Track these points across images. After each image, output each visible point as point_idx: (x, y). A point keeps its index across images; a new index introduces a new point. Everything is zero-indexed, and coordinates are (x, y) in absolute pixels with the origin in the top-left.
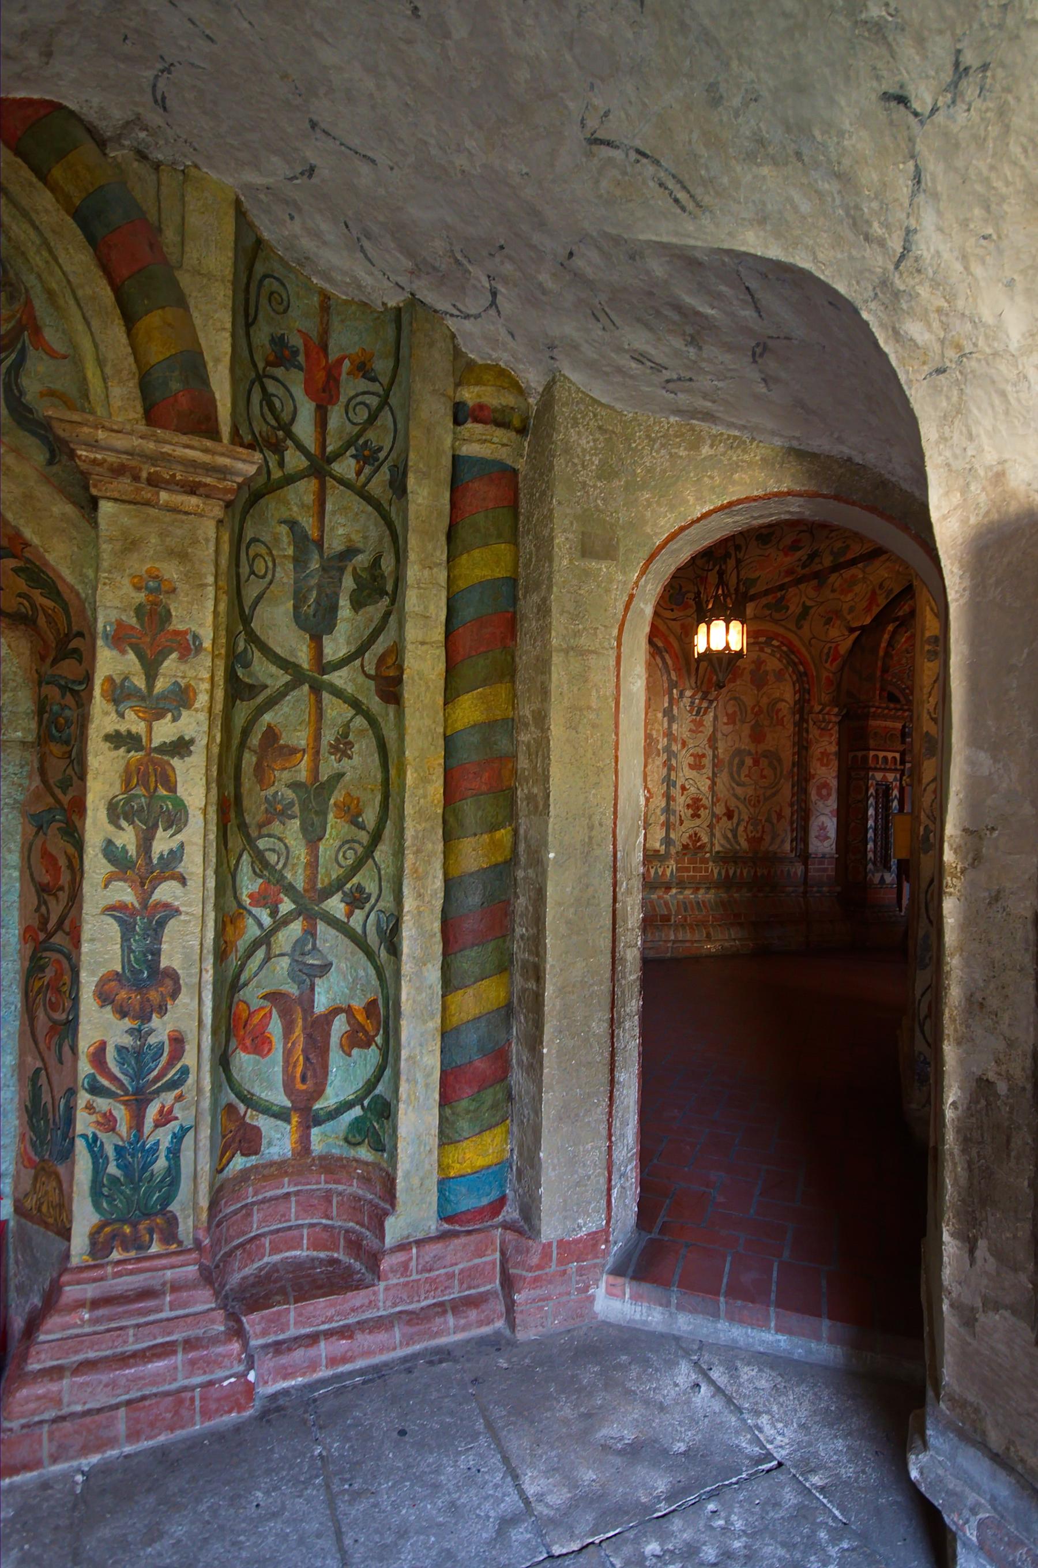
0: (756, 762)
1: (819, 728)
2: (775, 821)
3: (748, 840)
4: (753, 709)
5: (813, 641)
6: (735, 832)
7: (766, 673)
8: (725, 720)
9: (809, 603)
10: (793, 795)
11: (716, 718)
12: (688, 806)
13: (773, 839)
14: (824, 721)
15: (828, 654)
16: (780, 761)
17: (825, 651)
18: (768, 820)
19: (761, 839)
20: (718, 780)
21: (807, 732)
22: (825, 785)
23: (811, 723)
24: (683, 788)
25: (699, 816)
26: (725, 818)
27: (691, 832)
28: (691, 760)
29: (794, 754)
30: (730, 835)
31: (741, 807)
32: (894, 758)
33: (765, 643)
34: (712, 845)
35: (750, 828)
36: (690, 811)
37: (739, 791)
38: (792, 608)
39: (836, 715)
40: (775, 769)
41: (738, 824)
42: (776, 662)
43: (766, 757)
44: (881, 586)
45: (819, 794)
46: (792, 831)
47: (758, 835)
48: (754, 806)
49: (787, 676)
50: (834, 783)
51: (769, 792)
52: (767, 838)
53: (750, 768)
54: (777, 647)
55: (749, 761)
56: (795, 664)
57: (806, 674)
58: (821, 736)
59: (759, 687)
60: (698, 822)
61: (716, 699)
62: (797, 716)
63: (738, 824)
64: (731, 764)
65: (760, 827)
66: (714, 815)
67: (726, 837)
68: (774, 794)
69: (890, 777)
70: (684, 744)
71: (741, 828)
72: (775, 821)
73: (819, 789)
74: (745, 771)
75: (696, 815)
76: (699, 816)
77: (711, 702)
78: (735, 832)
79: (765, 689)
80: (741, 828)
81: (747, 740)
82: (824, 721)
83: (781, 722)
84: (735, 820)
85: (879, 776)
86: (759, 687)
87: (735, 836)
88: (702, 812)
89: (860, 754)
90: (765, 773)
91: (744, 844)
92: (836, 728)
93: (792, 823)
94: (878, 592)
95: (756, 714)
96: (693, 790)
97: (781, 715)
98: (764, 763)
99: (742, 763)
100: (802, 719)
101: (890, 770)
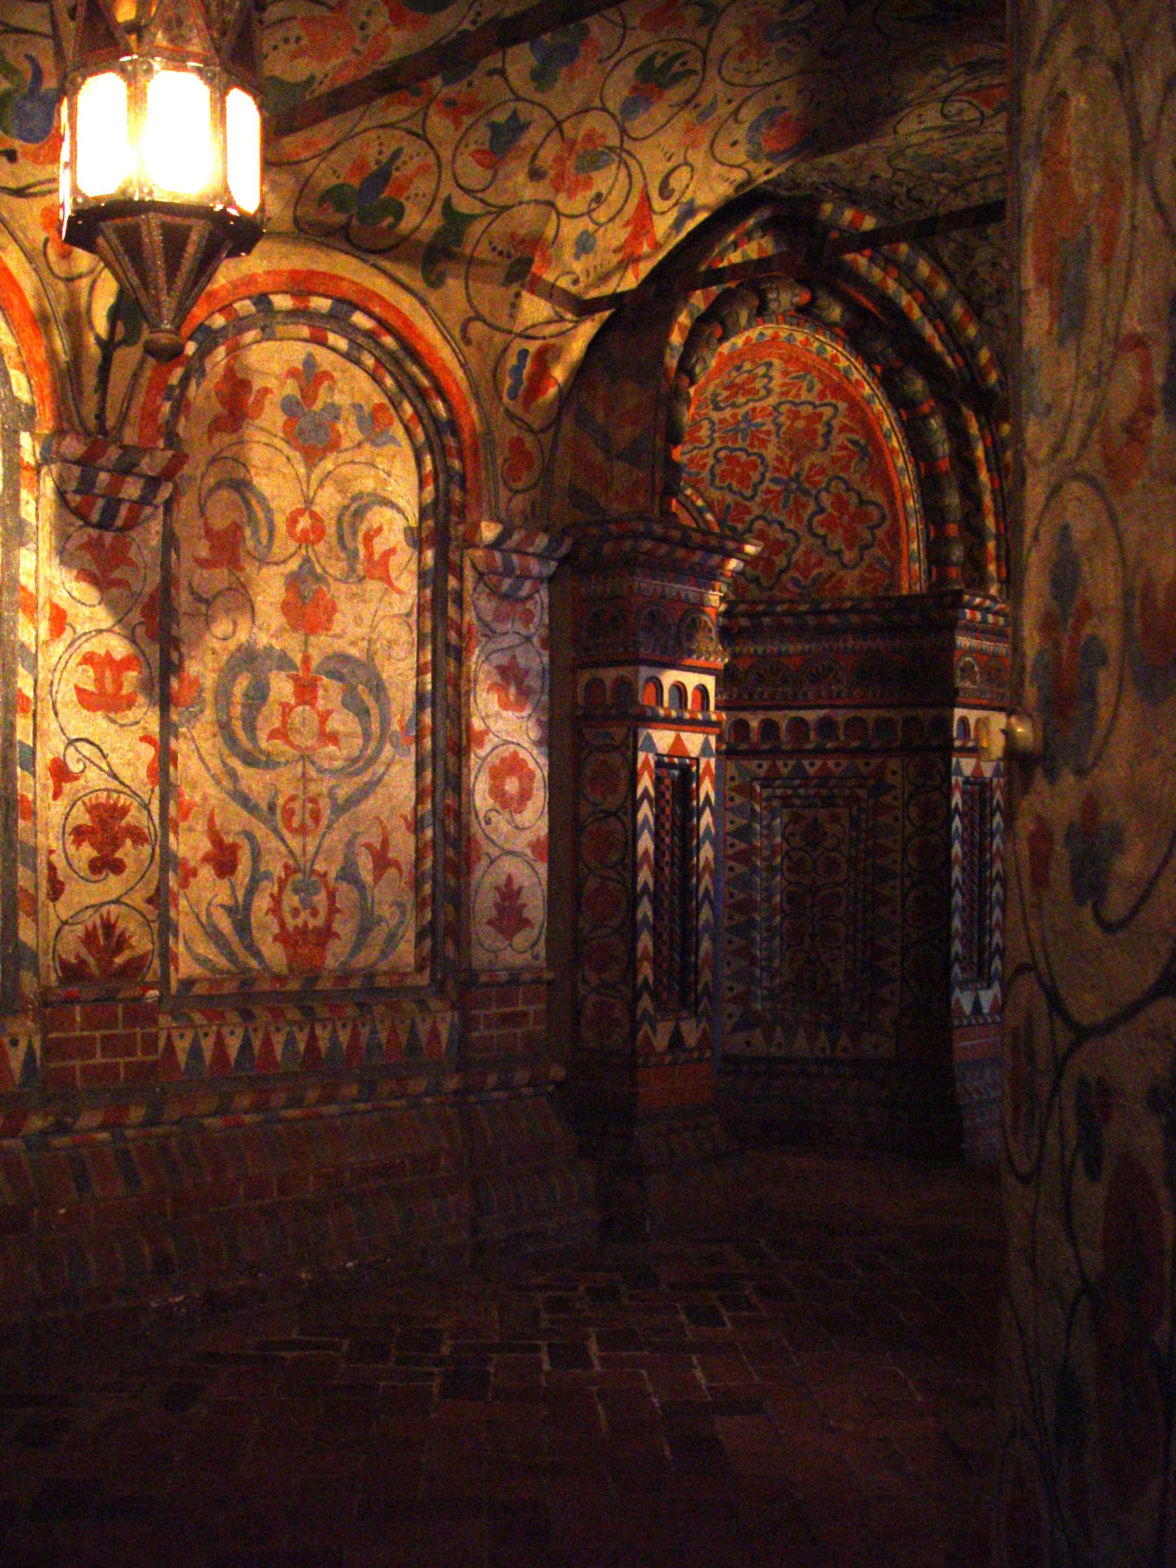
0: (306, 691)
1: (493, 593)
3: (284, 937)
4: (293, 521)
5: (477, 329)
6: (241, 915)
7: (334, 412)
8: (204, 553)
9: (464, 205)
10: (419, 799)
11: (170, 541)
12: (80, 834)
13: (364, 931)
14: (509, 570)
15: (517, 370)
16: (378, 688)
17: (512, 361)
18: (349, 874)
19: (326, 934)
20: (180, 746)
21: (460, 602)
22: (514, 765)
23: (469, 573)
24: (60, 772)
25: (118, 867)
26: (207, 872)
27: (93, 919)
28: (86, 678)
29: (420, 671)
30: (225, 924)
31: (261, 831)
32: (702, 690)
33: (332, 316)
34: (167, 957)
35: (291, 900)
36: (88, 851)
37: (253, 781)
39: (541, 557)
40: (363, 713)
41: (251, 892)
42: (364, 383)
45: (497, 792)
46: (420, 906)
47: (319, 922)
48: (302, 830)
49: (398, 431)
50: (537, 762)
52: (345, 928)
53: (286, 709)
54: (370, 334)
55: (282, 687)
56: (422, 393)
57: (453, 426)
58: (499, 617)
59: (312, 456)
60: (113, 885)
61: (169, 473)
62: (429, 554)
63: (251, 892)
64: (223, 694)
65: (321, 899)
66: (168, 860)
67: (215, 935)
69: (693, 742)
70: (59, 620)
71: (262, 903)
72: (367, 876)
73: (497, 775)
74: (270, 718)
75: (106, 864)
76: (118, 867)
77: (153, 483)
78: (241, 915)
79: (328, 464)
80: (262, 903)
81: (277, 620)
82: (509, 570)
83: (379, 568)
85: (663, 739)
86: (312, 456)
87: (243, 927)
88: (127, 852)
89: (610, 675)
90: (335, 724)
91: (274, 954)
92: (543, 595)
93: (417, 886)
94: (658, 204)
95: (304, 539)
96: (94, 778)
97: (379, 545)
98: (330, 693)
99: (259, 695)
100: (445, 566)
101: (693, 725)
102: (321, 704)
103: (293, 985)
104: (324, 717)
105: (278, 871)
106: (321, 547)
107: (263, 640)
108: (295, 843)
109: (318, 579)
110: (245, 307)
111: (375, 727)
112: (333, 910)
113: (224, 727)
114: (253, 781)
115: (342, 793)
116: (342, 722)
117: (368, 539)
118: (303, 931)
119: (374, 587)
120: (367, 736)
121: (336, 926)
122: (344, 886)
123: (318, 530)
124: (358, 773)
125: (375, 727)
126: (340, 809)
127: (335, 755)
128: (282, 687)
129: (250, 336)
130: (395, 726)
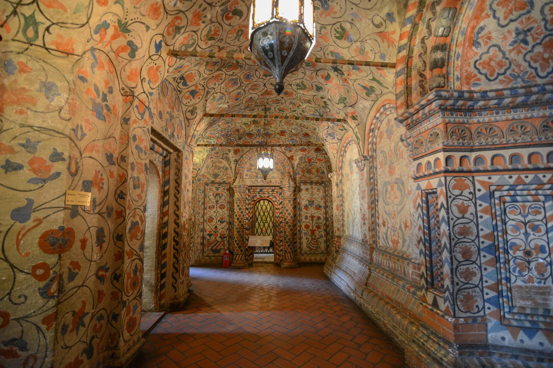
2: (404, 229)
13: (404, 242)
31: (388, 218)
38: (373, 85)
43: (396, 183)
44: (378, 26)
47: (396, 239)
48: (393, 218)
51: (400, 207)
52: (401, 241)
55: (389, 188)
63: (387, 230)
65: (396, 233)
68: (402, 209)
72: (404, 229)
74: (388, 195)
81: (387, 174)
84: (386, 227)
91: (390, 243)
102: (395, 190)
103: (391, 252)
104: (395, 193)
105: (391, 227)
106: (393, 157)
107: (387, 180)
108: (392, 221)
109: (393, 163)
110: (374, 121)
111: (403, 193)
112: (399, 237)
113: (383, 198)
114: (387, 208)
115: (399, 210)
116: (398, 194)
117: (399, 149)
118: (394, 240)
119: (401, 160)
120: (402, 195)
121: (399, 241)
122: (400, 231)
123: (392, 153)
124: (401, 205)
125: (403, 193)
126: (398, 213)
127: (397, 201)
128: (389, 188)
129: (379, 125)
130: (406, 192)
